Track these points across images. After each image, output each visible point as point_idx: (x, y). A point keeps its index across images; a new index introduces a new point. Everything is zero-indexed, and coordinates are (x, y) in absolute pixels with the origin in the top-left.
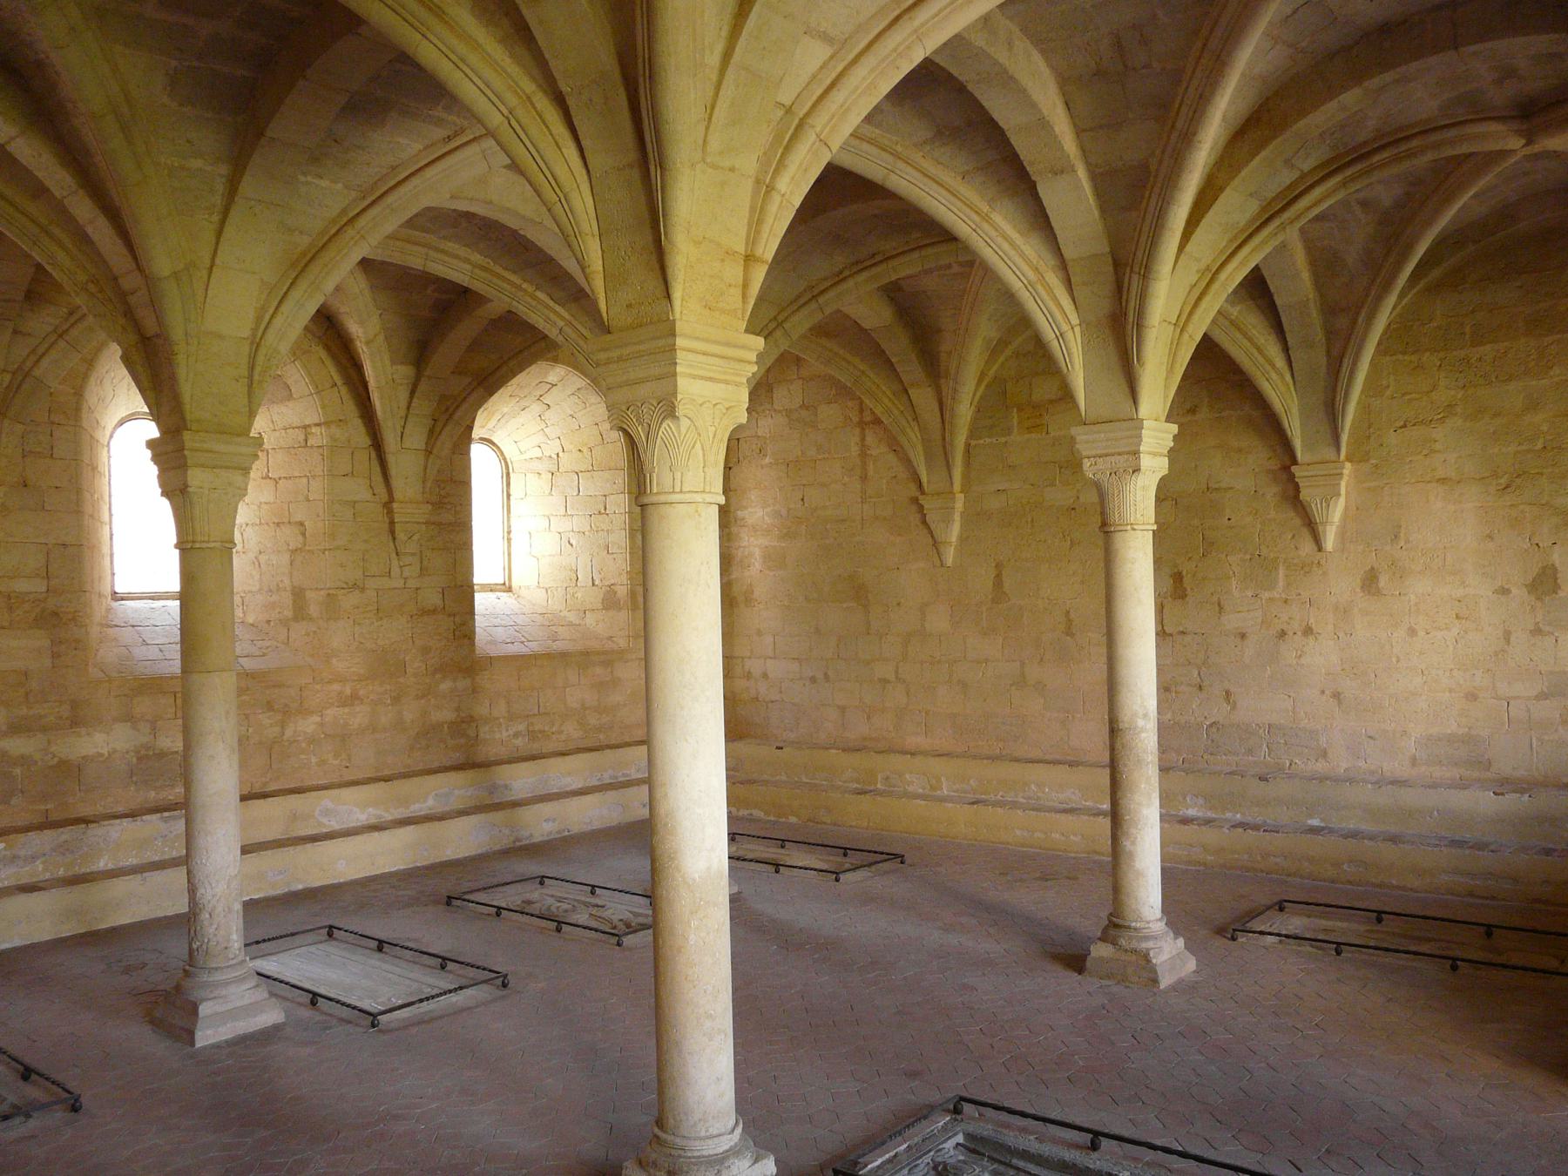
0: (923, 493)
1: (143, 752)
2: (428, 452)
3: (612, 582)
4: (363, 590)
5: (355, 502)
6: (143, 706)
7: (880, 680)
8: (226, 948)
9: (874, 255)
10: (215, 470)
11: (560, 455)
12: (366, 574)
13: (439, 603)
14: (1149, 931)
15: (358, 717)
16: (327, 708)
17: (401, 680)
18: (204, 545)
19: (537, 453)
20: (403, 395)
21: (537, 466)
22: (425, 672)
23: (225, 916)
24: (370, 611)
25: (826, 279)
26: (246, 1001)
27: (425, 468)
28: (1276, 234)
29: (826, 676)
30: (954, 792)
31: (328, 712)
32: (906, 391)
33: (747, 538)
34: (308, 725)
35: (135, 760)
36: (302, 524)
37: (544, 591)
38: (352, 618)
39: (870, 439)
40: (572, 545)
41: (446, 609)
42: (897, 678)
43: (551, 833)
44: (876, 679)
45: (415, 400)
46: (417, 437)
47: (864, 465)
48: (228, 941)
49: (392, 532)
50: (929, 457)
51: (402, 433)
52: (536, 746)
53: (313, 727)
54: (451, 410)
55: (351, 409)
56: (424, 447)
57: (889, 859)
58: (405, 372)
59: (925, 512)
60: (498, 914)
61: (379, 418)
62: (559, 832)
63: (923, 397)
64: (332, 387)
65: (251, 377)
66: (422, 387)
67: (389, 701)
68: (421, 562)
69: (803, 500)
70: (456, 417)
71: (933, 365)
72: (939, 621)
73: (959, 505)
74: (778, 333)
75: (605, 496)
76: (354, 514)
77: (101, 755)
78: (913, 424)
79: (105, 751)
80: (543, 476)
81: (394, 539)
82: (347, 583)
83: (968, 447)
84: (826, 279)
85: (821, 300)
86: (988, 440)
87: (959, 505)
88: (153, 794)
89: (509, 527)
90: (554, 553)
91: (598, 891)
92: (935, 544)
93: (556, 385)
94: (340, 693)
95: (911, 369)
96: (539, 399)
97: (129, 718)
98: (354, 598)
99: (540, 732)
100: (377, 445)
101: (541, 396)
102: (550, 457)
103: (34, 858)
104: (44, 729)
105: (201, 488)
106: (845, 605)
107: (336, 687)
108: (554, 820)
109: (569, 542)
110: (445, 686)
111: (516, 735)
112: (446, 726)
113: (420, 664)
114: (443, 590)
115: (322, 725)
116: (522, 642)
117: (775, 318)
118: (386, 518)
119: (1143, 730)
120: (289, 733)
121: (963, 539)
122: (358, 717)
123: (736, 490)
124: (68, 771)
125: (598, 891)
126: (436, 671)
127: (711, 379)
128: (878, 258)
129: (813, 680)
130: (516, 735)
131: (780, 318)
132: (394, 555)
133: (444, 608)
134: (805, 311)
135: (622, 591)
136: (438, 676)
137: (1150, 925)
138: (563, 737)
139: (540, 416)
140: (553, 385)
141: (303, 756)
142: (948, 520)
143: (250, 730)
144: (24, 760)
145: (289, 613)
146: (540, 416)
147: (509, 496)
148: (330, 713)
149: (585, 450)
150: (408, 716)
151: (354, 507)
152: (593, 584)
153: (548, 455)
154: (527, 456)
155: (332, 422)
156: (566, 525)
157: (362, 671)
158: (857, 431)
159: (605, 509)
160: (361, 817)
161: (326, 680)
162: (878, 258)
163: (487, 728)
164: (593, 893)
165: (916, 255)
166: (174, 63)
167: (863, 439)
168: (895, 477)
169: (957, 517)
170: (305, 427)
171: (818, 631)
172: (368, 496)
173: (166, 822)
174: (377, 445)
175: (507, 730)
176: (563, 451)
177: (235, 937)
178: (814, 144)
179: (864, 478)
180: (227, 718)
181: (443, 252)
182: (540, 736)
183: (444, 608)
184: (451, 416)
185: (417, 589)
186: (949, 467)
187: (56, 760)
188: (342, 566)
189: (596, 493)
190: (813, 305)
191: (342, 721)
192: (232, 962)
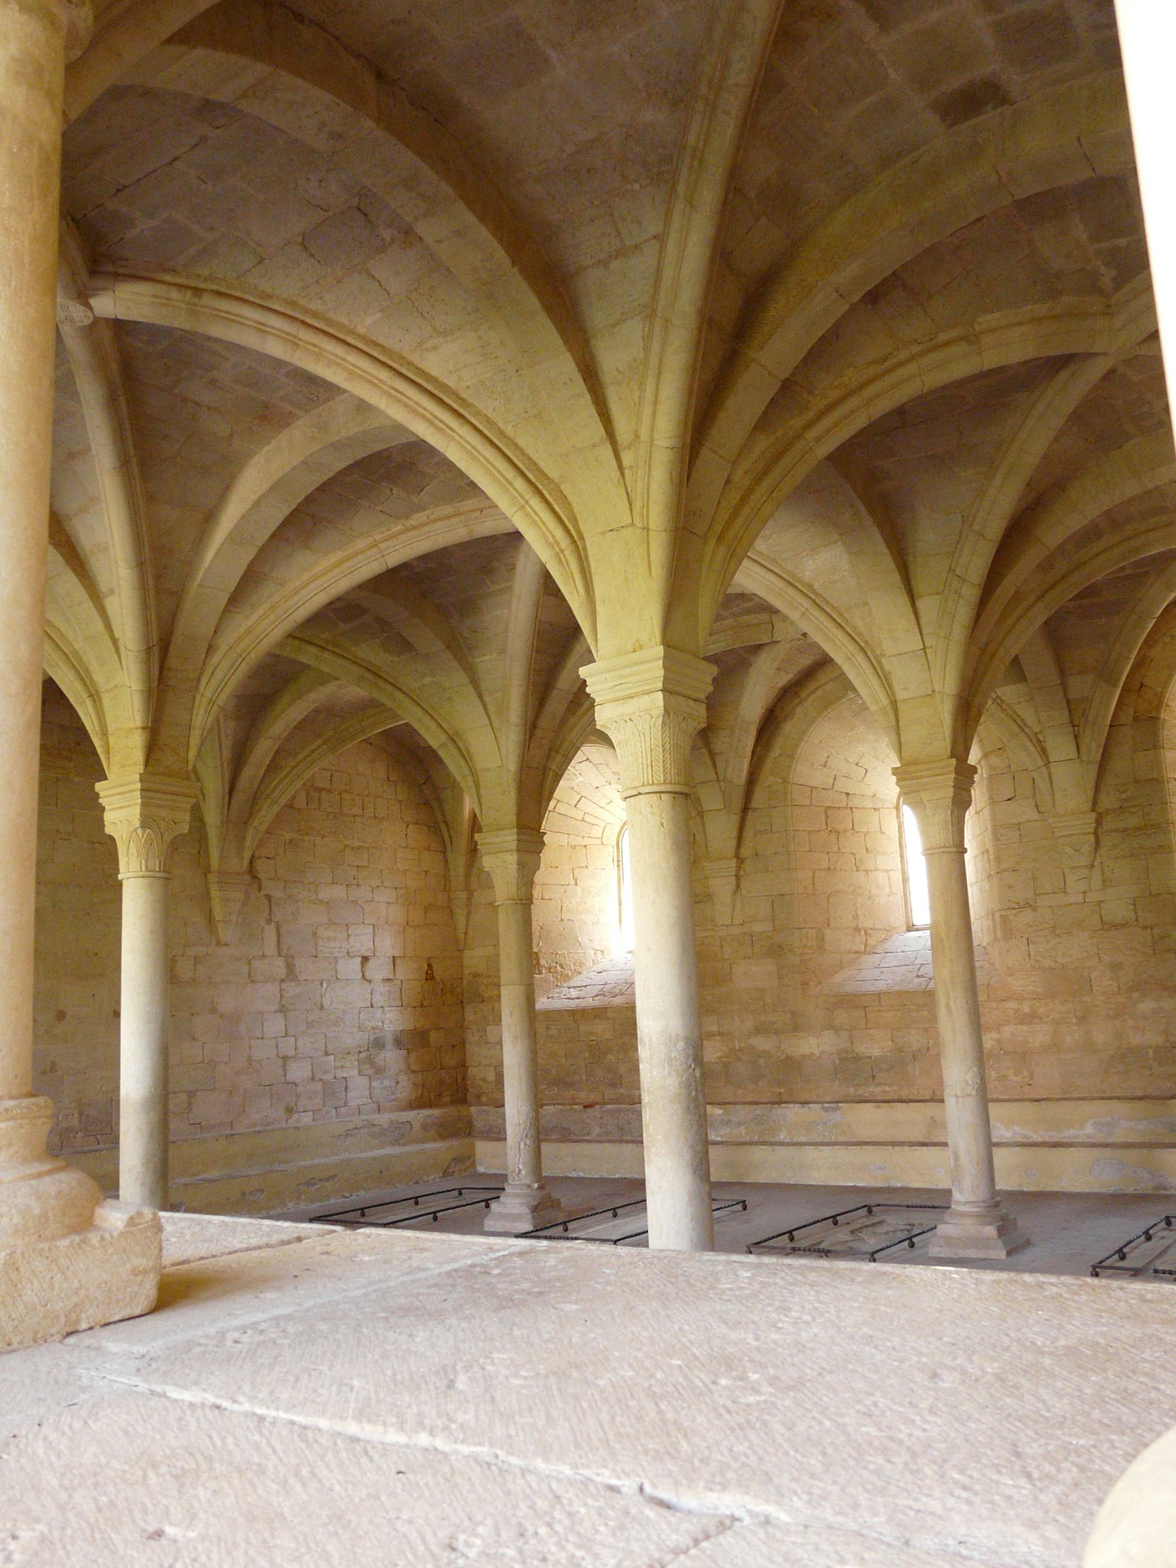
1: (843, 1055)
4: (1035, 909)
5: (1019, 824)
6: (842, 1017)
12: (1037, 892)
13: (1132, 915)
15: (1039, 1036)
16: (1002, 1025)
17: (1087, 999)
22: (1117, 990)
24: (1045, 929)
26: (516, 1211)
31: (1006, 1028)
35: (837, 1061)
38: (1025, 936)
41: (1140, 920)
56: (1074, 755)
67: (1074, 1020)
68: (1103, 875)
77: (812, 1054)
79: (817, 1052)
88: (852, 1090)
94: (1018, 1010)
97: (831, 1026)
98: (1027, 917)
103: (740, 1124)
104: (776, 1032)
107: (1012, 1005)
112: (1151, 1051)
113: (1110, 982)
115: (999, 1041)
122: (1039, 1036)
124: (791, 1064)
126: (1131, 989)
133: (1137, 920)
136: (1136, 995)
143: (931, 1042)
144: (765, 1054)
148: (1007, 1030)
151: (1019, 829)
157: (1039, 990)
166: (377, 640)
173: (826, 1111)
185: (1100, 902)
187: (784, 1056)
188: (1010, 887)
191: (1021, 1039)
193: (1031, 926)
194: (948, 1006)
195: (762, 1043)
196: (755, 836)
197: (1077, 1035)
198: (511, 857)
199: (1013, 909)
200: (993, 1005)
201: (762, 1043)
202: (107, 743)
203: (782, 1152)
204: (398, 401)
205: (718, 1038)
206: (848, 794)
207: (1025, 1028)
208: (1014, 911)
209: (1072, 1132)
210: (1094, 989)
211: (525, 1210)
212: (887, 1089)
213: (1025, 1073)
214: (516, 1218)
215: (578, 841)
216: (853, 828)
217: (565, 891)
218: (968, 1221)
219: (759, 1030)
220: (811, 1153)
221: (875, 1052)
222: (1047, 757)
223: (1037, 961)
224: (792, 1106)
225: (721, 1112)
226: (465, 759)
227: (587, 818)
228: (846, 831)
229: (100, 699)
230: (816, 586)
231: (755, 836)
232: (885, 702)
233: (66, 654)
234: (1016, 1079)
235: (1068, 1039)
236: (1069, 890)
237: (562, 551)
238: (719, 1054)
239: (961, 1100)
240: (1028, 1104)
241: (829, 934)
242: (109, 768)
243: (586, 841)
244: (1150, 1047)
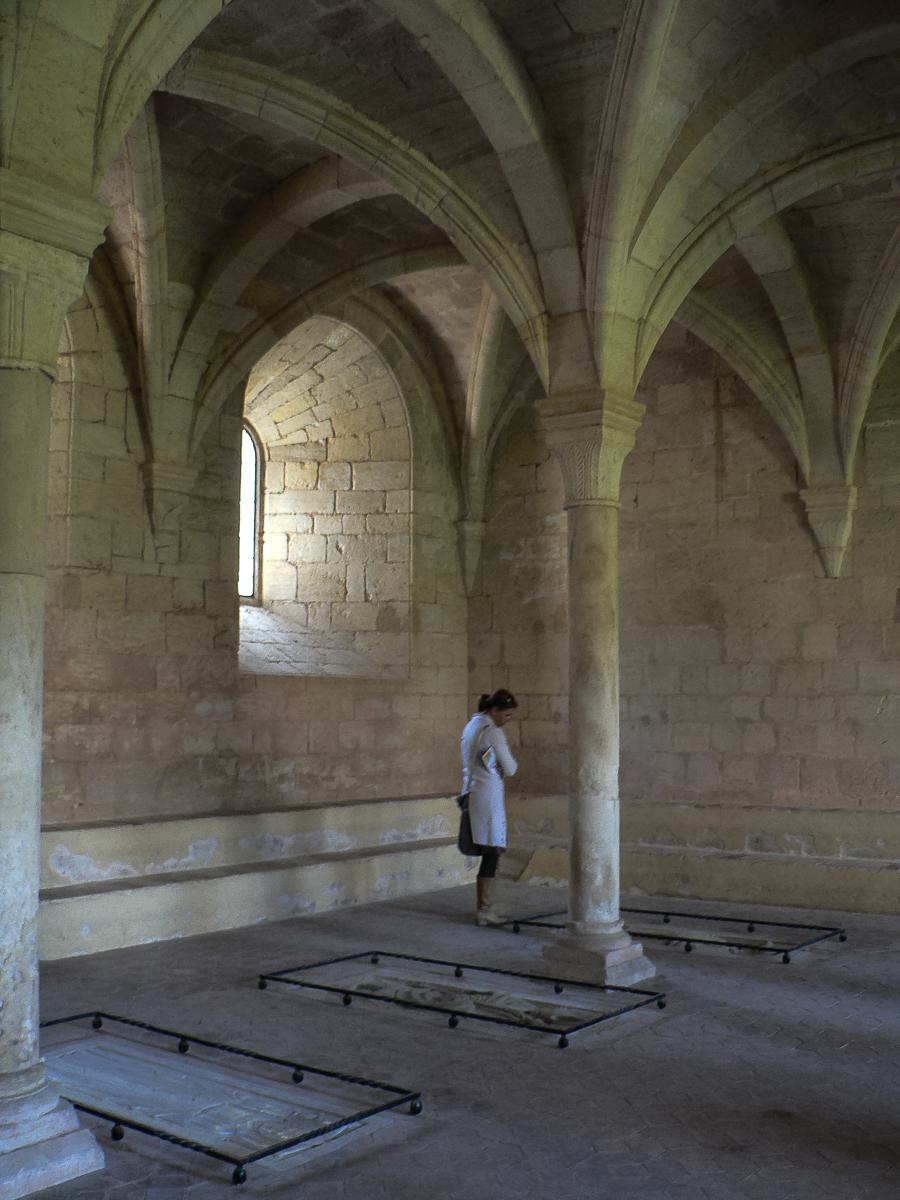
0: (805, 486)
2: (199, 402)
3: (391, 597)
4: (110, 572)
5: (105, 458)
7: (738, 720)
8: (15, 1042)
9: (838, 140)
10: (40, 245)
11: (330, 440)
17: (150, 695)
18: (15, 363)
19: (301, 437)
20: (175, 322)
21: (298, 453)
23: (14, 989)
25: (780, 164)
27: (193, 424)
29: (665, 718)
30: (854, 856)
32: (790, 359)
33: (558, 549)
37: (302, 606)
39: (729, 425)
40: (340, 551)
42: (762, 716)
44: (733, 718)
45: (190, 333)
46: (185, 383)
47: (721, 457)
48: (20, 1030)
49: (149, 502)
50: (814, 442)
51: (170, 375)
54: (230, 352)
55: (106, 340)
56: (192, 395)
57: (826, 937)
58: (181, 292)
59: (807, 510)
60: (347, 1002)
61: (146, 349)
63: (815, 368)
64: (87, 308)
65: (101, 112)
66: (200, 314)
68: (180, 546)
69: (635, 500)
70: (237, 359)
71: (834, 328)
72: (821, 644)
73: (852, 501)
74: (723, 227)
75: (385, 491)
76: (104, 474)
78: (797, 401)
80: (307, 466)
81: (150, 512)
82: (91, 562)
83: (864, 430)
84: (780, 164)
85: (776, 189)
86: (890, 423)
87: (852, 501)
89: (262, 527)
90: (316, 559)
91: (465, 971)
92: (819, 550)
93: (336, 350)
94: (77, 705)
95: (803, 329)
96: (312, 368)
100: (137, 389)
101: (316, 364)
102: (317, 442)
105: (16, 268)
106: (691, 628)
107: (71, 697)
109: (337, 547)
110: (203, 707)
112: (201, 760)
114: (204, 584)
116: (288, 663)
117: (719, 206)
118: (141, 483)
121: (856, 544)
123: (544, 491)
125: (465, 971)
128: (844, 144)
129: (646, 720)
131: (726, 207)
132: (148, 532)
133: (204, 607)
134: (753, 203)
135: (402, 609)
136: (194, 694)
138: (334, 785)
139: (310, 390)
140: (332, 351)
142: (838, 520)
146: (310, 390)
147: (263, 489)
149: (362, 436)
150: (157, 744)
151: (104, 465)
152: (366, 600)
153: (314, 440)
154: (287, 441)
155: (84, 352)
156: (333, 526)
158: (711, 416)
159: (384, 508)
161: (60, 687)
162: (844, 144)
163: (248, 767)
164: (458, 974)
165: (888, 145)
167: (719, 424)
168: (763, 470)
169: (849, 516)
171: (653, 661)
172: (121, 452)
174: (137, 389)
176: (334, 436)
179: (720, 473)
180: (31, 652)
181: (289, 90)
182: (308, 781)
183: (204, 607)
184: (229, 360)
185: (174, 579)
186: (841, 453)
189: (374, 488)
190: (765, 196)
191: (77, 743)
192: (23, 1066)
197: (135, 740)
199: (86, 568)
207: (83, 729)
208: (86, 571)
210: (159, 683)
213: (76, 791)
214: (53, 1147)
234: (67, 797)
235: (127, 744)
236: (146, 557)
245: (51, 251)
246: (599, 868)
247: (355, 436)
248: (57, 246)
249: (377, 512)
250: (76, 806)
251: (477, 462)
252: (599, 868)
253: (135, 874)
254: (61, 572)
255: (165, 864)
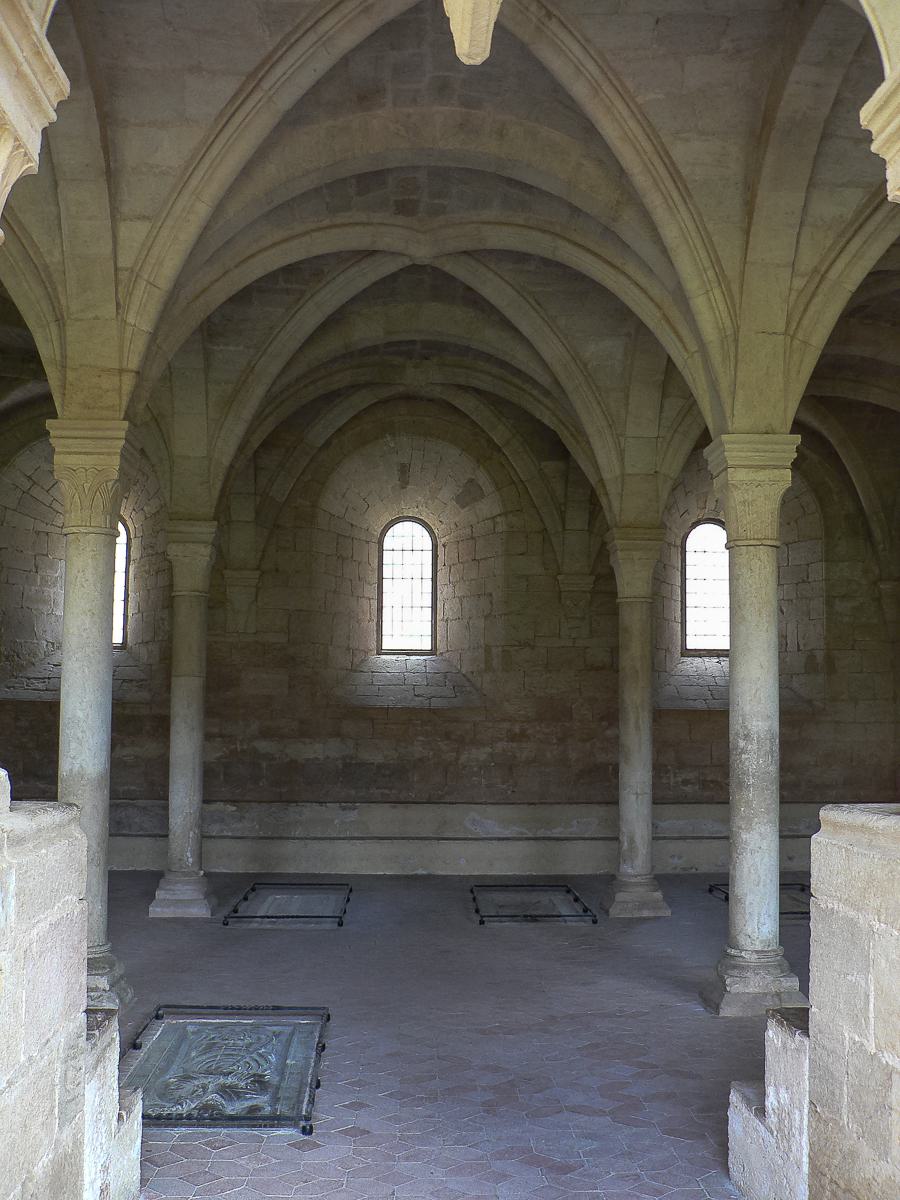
1: (348, 761)
4: (533, 648)
14: (741, 959)
17: (567, 724)
28: (894, 217)
34: (482, 754)
35: (341, 766)
36: (491, 595)
43: (675, 868)
52: (707, 793)
53: (485, 756)
62: (684, 869)
67: (555, 741)
77: (317, 759)
88: (353, 792)
99: (712, 782)
107: (506, 725)
108: (680, 858)
111: (685, 782)
119: (744, 751)
120: (463, 758)
126: (602, 719)
127: (85, 453)
130: (685, 782)
135: (820, 656)
136: (604, 723)
137: (743, 954)
141: (475, 778)
145: (482, 666)
148: (500, 746)
150: (573, 755)
152: (799, 650)
160: (498, 831)
170: (493, 518)
175: (675, 776)
177: (189, 854)
178: (145, 288)
191: (510, 754)
193: (527, 661)
194: (637, 722)
195: (263, 746)
196: (277, 551)
198: (203, 549)
200: (490, 725)
201: (263, 746)
202: (65, 377)
203: (316, 846)
204: (650, 172)
205: (219, 739)
206: (352, 525)
207: (514, 745)
208: (516, 648)
209: (559, 829)
211: (202, 897)
212: (387, 791)
215: (41, 527)
216: (352, 557)
217: (27, 577)
218: (641, 890)
219: (265, 734)
220: (344, 847)
221: (378, 759)
222: (564, 526)
223: (530, 691)
224: (308, 804)
225: (234, 808)
226: (166, 443)
227: (56, 506)
228: (347, 559)
229: (64, 325)
230: (589, 367)
231: (277, 551)
232: (618, 472)
233: (36, 267)
235: (549, 755)
237: (726, 336)
238: (218, 755)
239: (640, 797)
240: (526, 806)
241: (330, 648)
242: (62, 406)
243: (49, 528)
244: (611, 764)
245: (192, 546)
246: (625, 838)
247: (789, 524)
248: (193, 542)
249: (804, 581)
250: (509, 792)
251: (878, 534)
252: (625, 838)
253: (530, 835)
254: (500, 649)
255: (554, 831)
